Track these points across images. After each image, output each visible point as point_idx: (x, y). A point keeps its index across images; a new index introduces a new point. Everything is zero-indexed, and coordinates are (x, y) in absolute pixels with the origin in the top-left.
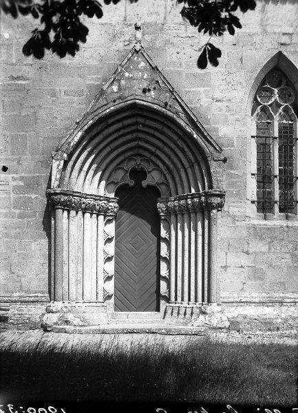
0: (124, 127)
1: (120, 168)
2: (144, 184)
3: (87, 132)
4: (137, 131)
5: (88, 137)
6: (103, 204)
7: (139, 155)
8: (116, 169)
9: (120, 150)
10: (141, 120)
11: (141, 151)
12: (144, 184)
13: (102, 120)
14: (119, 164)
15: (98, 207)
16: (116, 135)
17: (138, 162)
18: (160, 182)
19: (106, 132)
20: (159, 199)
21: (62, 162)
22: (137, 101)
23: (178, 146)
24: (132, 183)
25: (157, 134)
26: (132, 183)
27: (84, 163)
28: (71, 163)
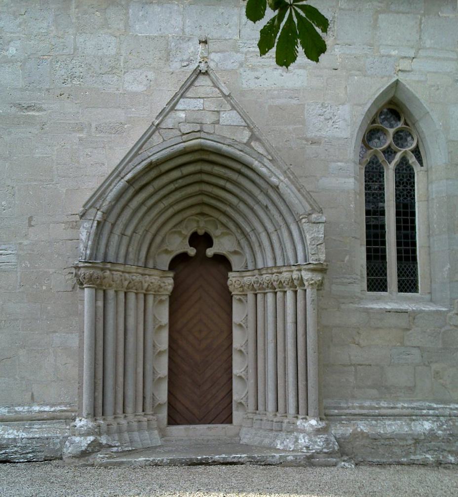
0: (183, 177)
1: (175, 232)
2: (210, 252)
3: (131, 182)
4: (202, 182)
5: (131, 191)
6: (153, 281)
7: (202, 214)
8: (173, 232)
9: (177, 208)
10: (207, 167)
11: (206, 210)
12: (210, 252)
13: (151, 166)
14: (175, 226)
15: (146, 285)
16: (172, 187)
17: (202, 224)
18: (233, 250)
19: (158, 184)
20: (230, 274)
21: (95, 224)
22: (202, 141)
23: (258, 202)
24: (192, 252)
25: (229, 186)
26: (192, 252)
27: (126, 226)
28: (108, 226)
